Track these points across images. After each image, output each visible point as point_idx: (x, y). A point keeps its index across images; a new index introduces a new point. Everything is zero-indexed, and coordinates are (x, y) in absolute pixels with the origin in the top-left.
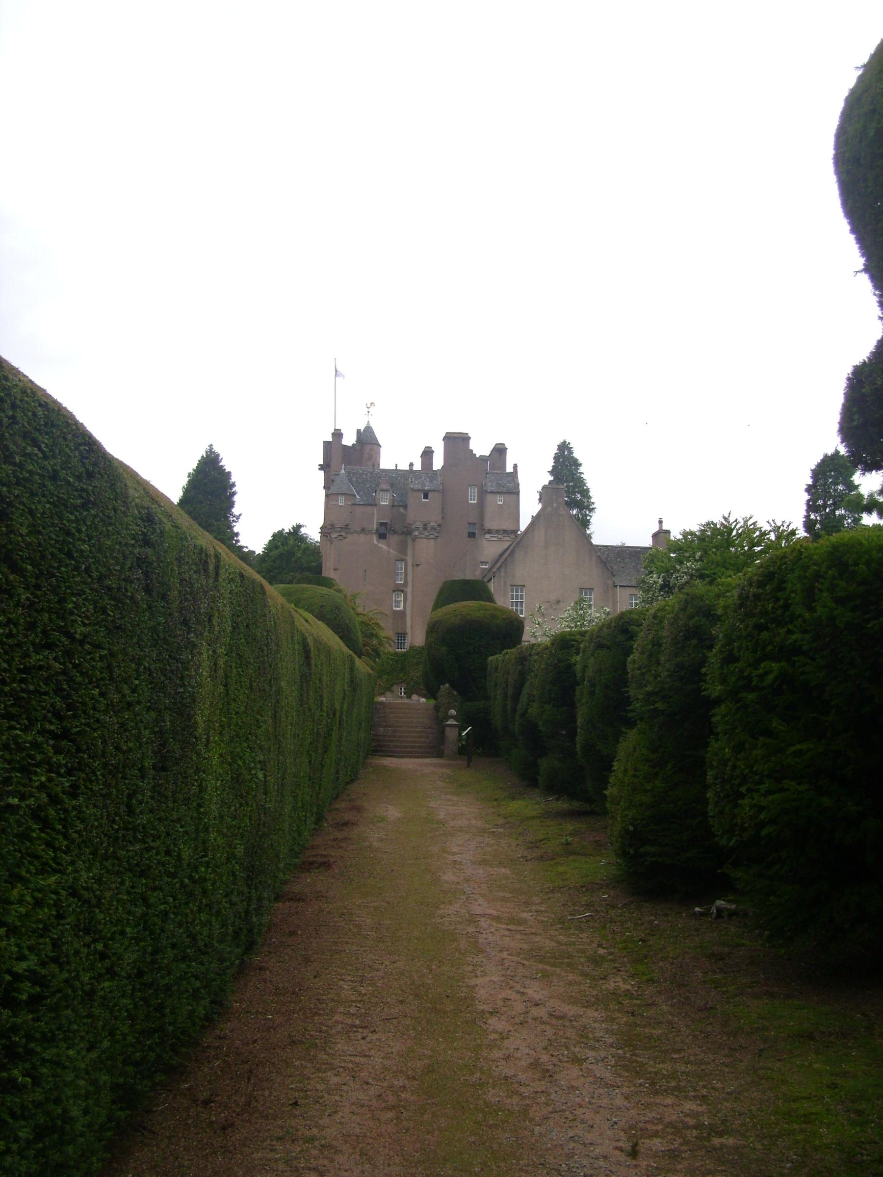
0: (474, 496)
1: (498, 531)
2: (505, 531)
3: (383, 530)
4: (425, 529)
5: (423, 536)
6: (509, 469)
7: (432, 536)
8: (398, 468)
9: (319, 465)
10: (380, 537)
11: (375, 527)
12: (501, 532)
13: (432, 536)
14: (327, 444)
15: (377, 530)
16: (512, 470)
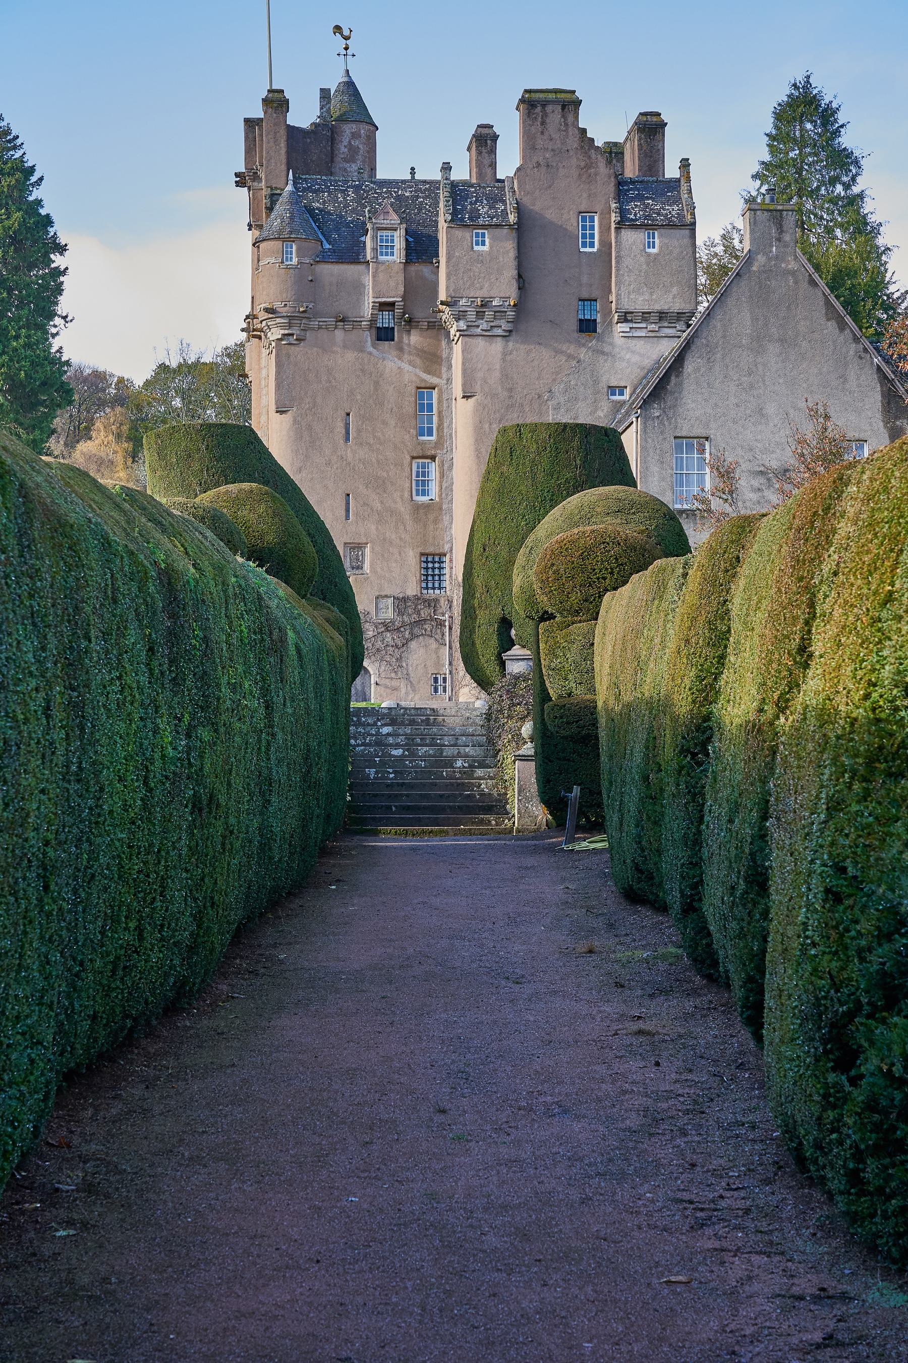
0: (592, 236)
1: (645, 316)
2: (662, 316)
3: (386, 320)
4: (480, 315)
5: (478, 331)
6: (671, 171)
7: (499, 332)
8: (417, 177)
9: (237, 175)
10: (379, 339)
11: (367, 310)
12: (654, 318)
13: (499, 332)
14: (250, 124)
15: (373, 321)
16: (677, 174)
